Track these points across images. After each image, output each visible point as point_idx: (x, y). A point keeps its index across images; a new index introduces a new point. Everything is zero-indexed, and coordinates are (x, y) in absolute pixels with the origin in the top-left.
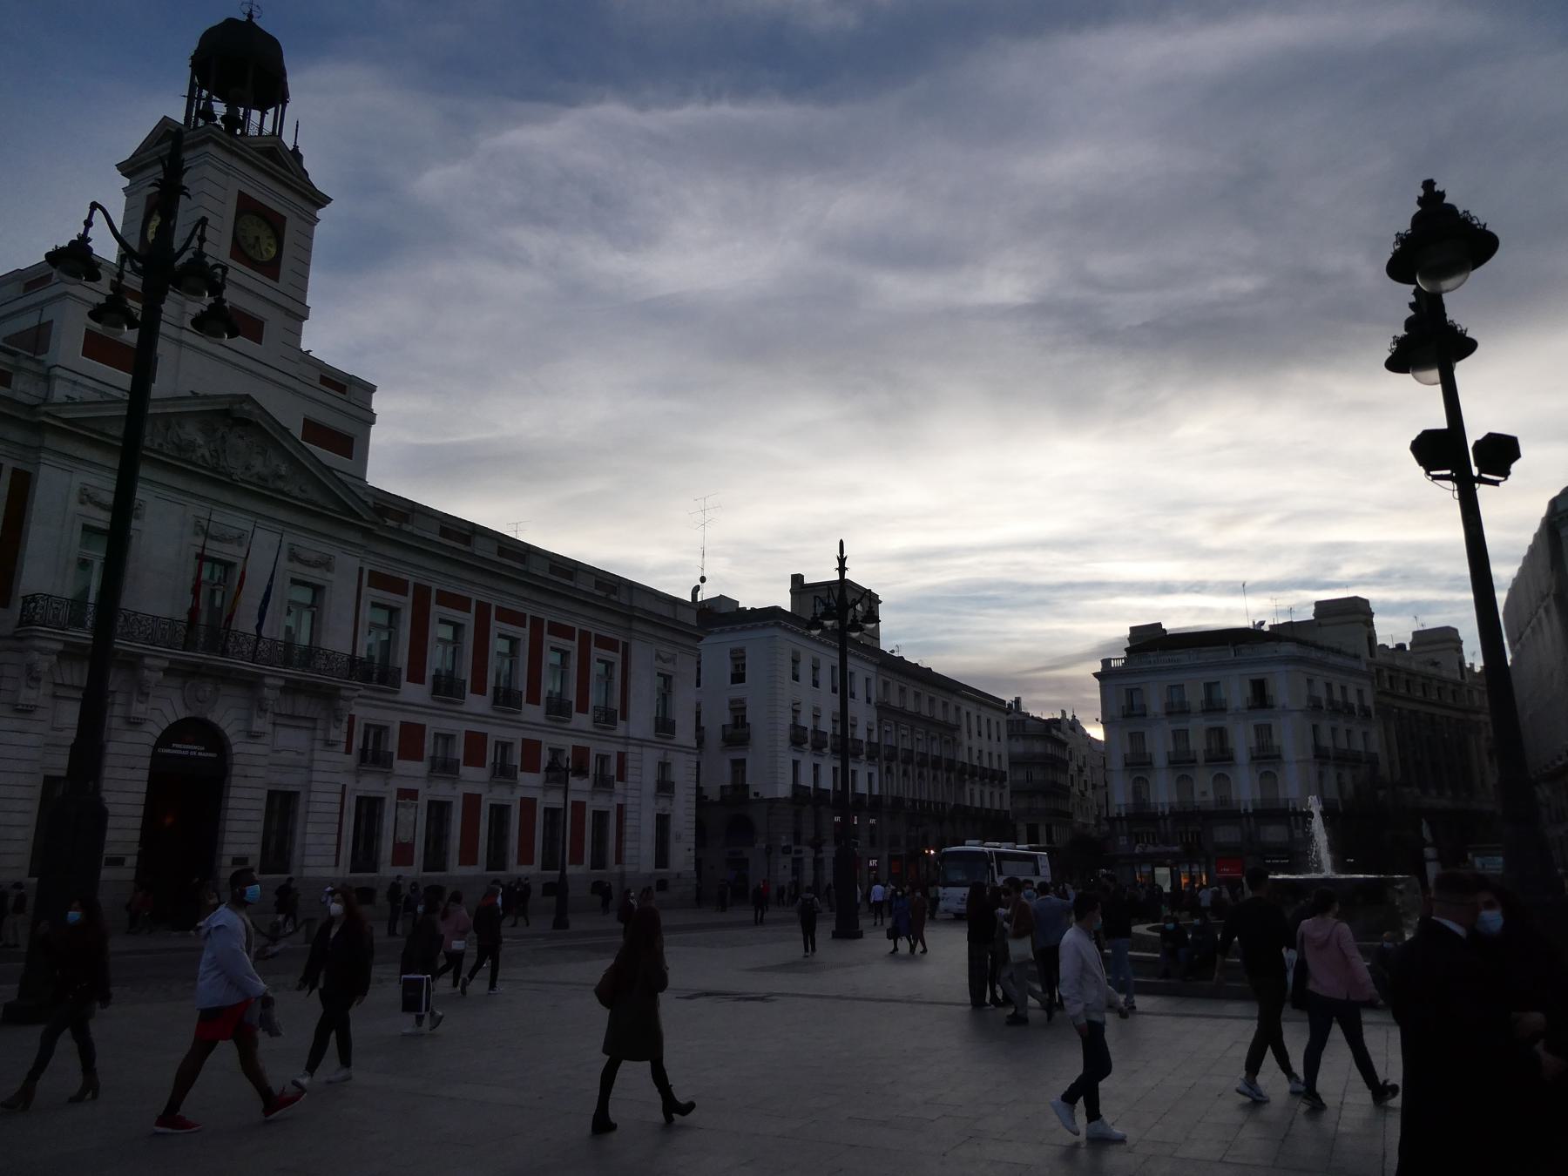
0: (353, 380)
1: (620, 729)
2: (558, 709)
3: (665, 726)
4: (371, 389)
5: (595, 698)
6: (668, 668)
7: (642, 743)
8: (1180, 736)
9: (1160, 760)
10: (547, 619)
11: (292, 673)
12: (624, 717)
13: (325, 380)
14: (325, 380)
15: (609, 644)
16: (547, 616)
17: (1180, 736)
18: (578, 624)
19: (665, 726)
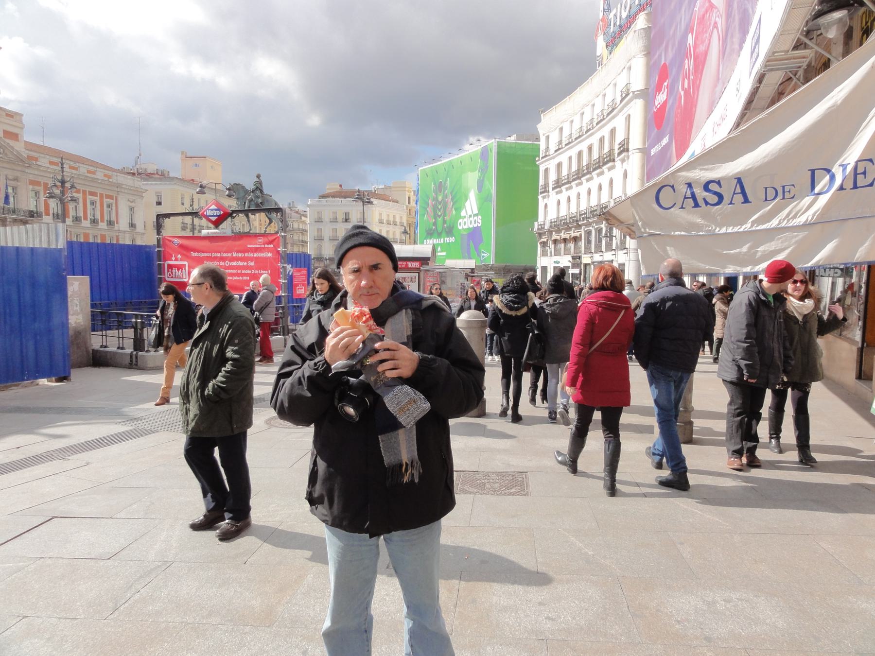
0: (16, 113)
1: (116, 227)
2: (94, 221)
3: (132, 226)
4: (22, 115)
5: (106, 218)
6: (132, 205)
7: (125, 232)
8: (335, 230)
9: (326, 238)
10: (87, 190)
11: (15, 216)
12: (117, 223)
13: (7, 115)
14: (7, 115)
15: (111, 197)
16: (88, 189)
17: (335, 230)
18: (99, 191)
19: (132, 226)
